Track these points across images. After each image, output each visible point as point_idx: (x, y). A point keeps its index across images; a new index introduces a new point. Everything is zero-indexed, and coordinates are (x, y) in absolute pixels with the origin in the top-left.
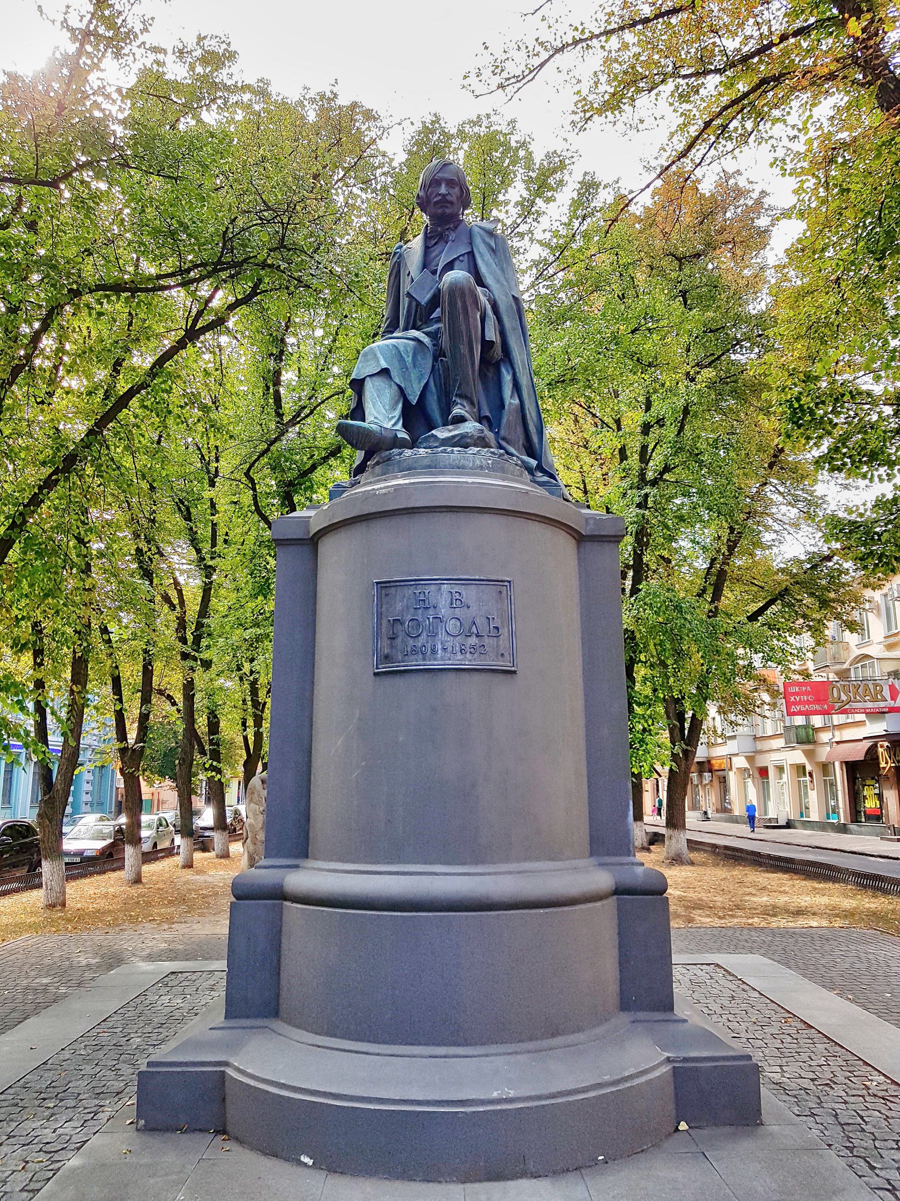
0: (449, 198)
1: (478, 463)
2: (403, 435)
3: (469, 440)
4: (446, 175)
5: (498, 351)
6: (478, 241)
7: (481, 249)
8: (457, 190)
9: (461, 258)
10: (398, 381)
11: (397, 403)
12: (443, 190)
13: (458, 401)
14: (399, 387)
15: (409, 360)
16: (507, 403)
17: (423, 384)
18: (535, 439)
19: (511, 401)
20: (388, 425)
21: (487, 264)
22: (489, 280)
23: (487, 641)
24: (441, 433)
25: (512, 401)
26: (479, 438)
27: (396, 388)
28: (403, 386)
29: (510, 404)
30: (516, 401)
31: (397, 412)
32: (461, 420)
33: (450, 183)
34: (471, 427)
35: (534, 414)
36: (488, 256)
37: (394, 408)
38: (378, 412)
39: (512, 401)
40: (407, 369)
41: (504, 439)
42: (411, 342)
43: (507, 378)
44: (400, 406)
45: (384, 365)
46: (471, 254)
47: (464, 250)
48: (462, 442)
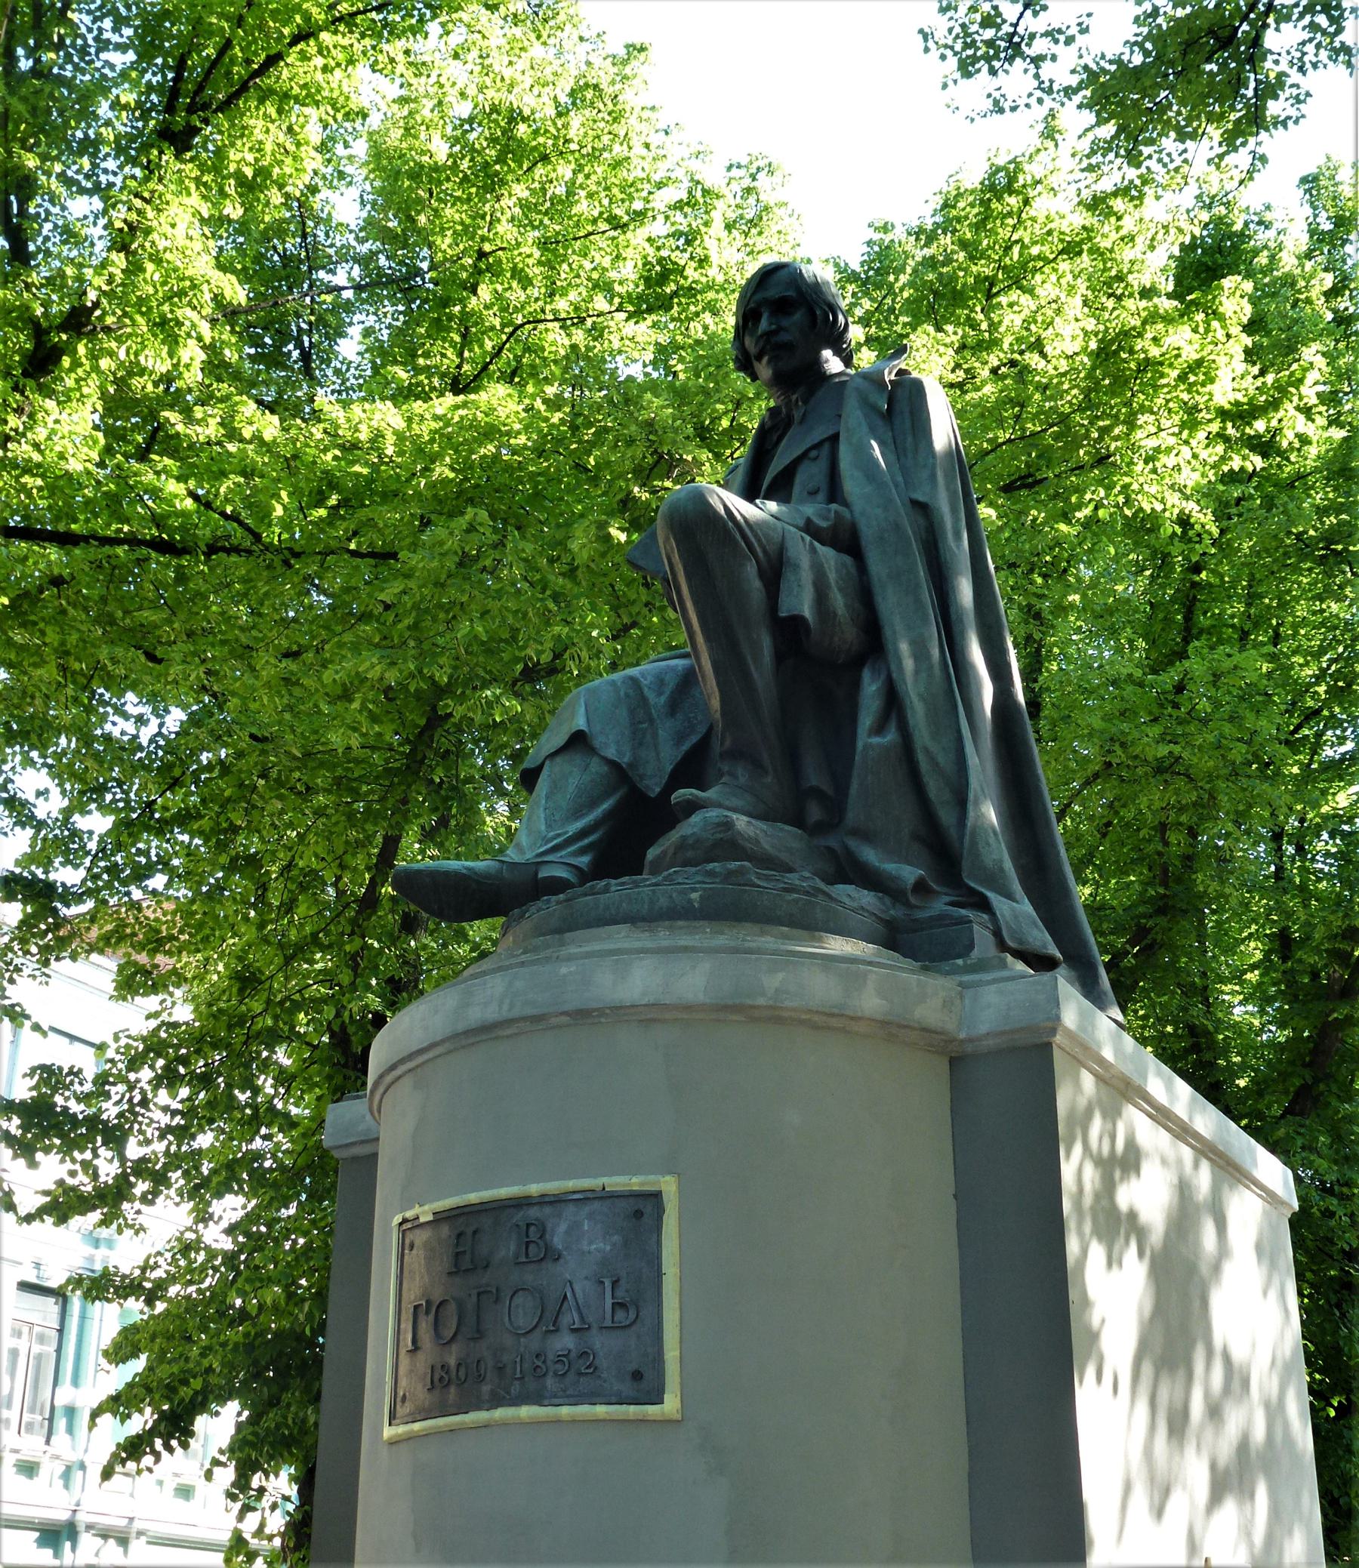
0: (784, 337)
1: (663, 902)
4: (772, 293)
5: (848, 634)
8: (798, 316)
9: (813, 454)
10: (611, 753)
11: (593, 804)
12: (764, 324)
14: (613, 764)
15: (658, 701)
16: (860, 745)
17: (686, 746)
18: (946, 816)
19: (871, 741)
22: (852, 484)
23: (599, 1342)
26: (717, 844)
28: (625, 760)
29: (867, 747)
31: (579, 825)
33: (781, 307)
35: (945, 760)
37: (576, 814)
39: (875, 740)
40: (651, 721)
41: (855, 832)
43: (871, 688)
44: (606, 806)
45: (580, 723)
46: (835, 439)
47: (819, 433)
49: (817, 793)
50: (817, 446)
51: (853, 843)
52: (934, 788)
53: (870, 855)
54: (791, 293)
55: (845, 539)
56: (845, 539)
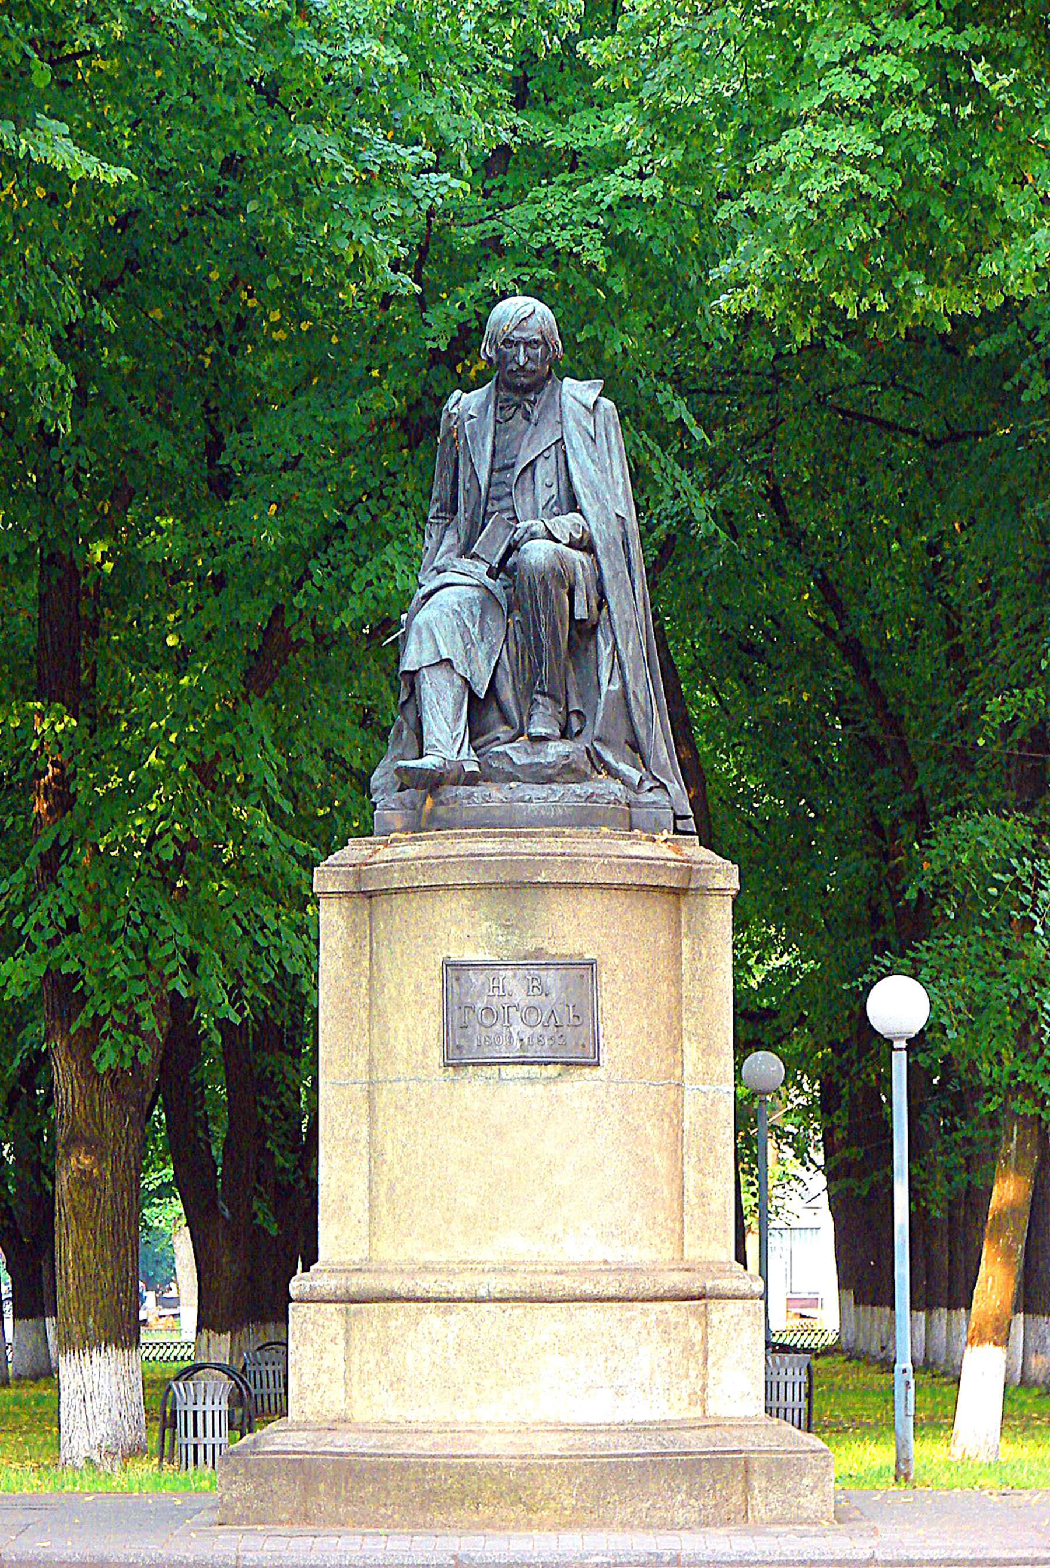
2: (472, 767)
3: (550, 772)
6: (570, 424)
7: (576, 441)
9: (546, 454)
13: (540, 698)
15: (475, 630)
18: (642, 732)
19: (609, 686)
20: (452, 755)
21: (583, 469)
24: (518, 754)
25: (612, 688)
27: (459, 682)
28: (468, 677)
30: (616, 686)
32: (544, 739)
33: (529, 343)
34: (556, 750)
36: (583, 455)
38: (441, 731)
42: (475, 593)
43: (605, 651)
47: (548, 438)
48: (543, 776)
49: (579, 713)
50: (549, 448)
51: (598, 747)
52: (637, 717)
53: (609, 757)
54: (538, 337)
55: (586, 545)
56: (586, 545)
